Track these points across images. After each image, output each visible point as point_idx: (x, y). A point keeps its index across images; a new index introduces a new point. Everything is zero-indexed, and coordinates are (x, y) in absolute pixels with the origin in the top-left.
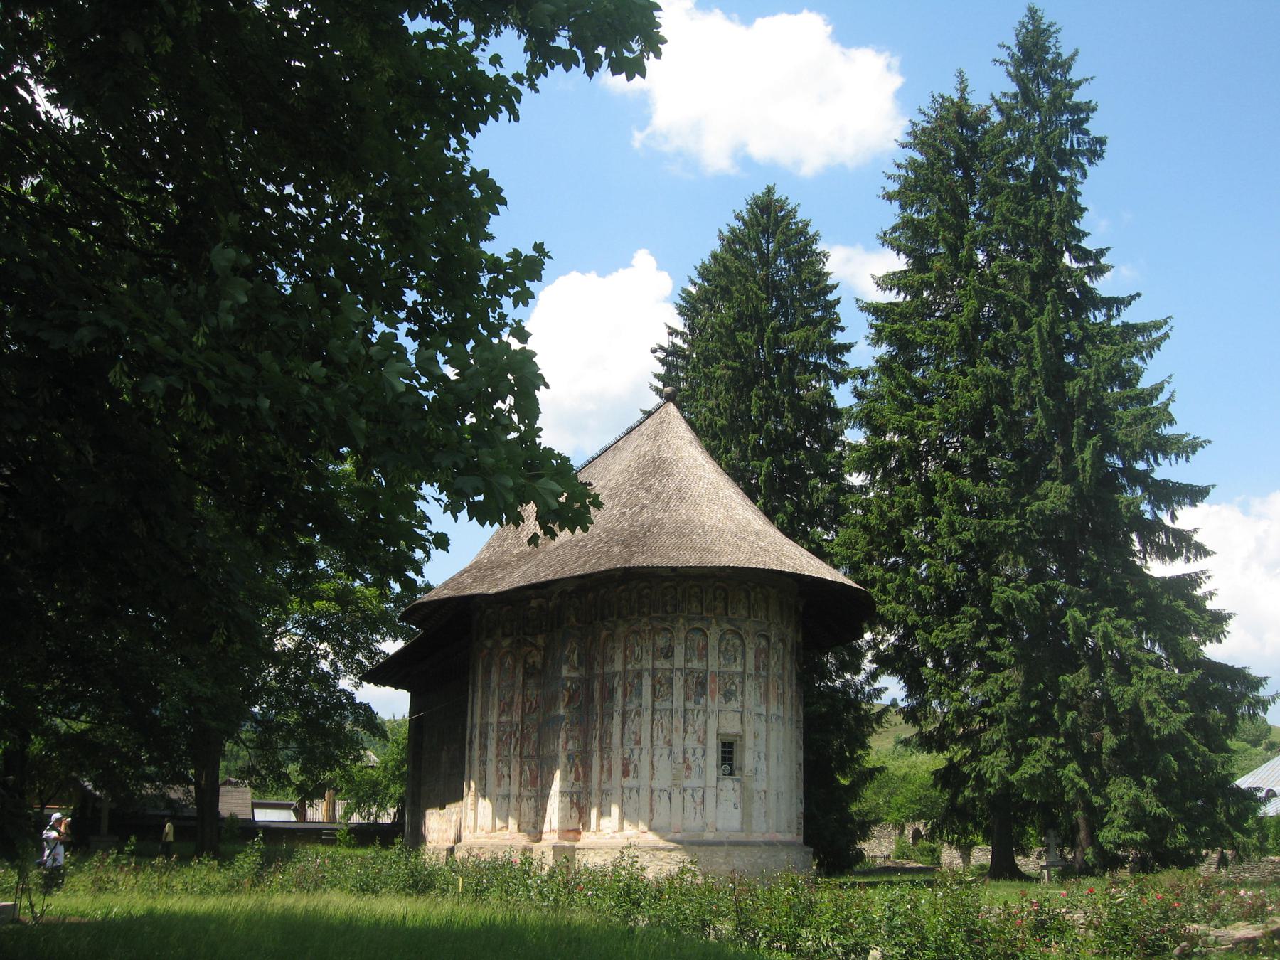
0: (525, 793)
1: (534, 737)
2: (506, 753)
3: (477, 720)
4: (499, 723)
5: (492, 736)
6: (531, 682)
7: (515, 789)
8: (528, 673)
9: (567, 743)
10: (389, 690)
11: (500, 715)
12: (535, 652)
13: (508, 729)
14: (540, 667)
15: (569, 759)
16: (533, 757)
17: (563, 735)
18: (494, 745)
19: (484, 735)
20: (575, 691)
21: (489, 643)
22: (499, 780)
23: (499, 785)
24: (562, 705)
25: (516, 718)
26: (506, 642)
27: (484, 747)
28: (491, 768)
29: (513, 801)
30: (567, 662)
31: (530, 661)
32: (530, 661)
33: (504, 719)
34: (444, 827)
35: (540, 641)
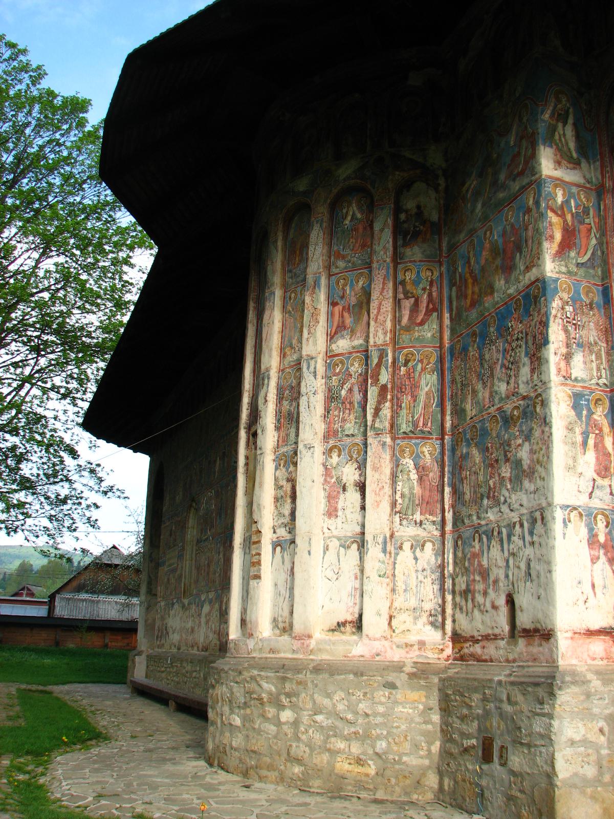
0: (408, 531)
1: (428, 383)
2: (351, 427)
3: (272, 361)
4: (330, 356)
5: (314, 387)
6: (415, 252)
7: (379, 519)
8: (404, 234)
9: (568, 357)
10: (127, 452)
11: (332, 337)
12: (420, 186)
13: (356, 368)
14: (435, 217)
15: (576, 407)
16: (425, 436)
17: (556, 334)
18: (320, 409)
19: (291, 393)
20: (580, 217)
21: (302, 185)
22: (331, 498)
23: (332, 512)
24: (549, 249)
25: (380, 336)
26: (346, 171)
27: (290, 420)
28: (311, 467)
29: (374, 552)
30: (550, 140)
31: (410, 204)
32: (410, 205)
33: (343, 344)
34: (189, 625)
35: (435, 157)
